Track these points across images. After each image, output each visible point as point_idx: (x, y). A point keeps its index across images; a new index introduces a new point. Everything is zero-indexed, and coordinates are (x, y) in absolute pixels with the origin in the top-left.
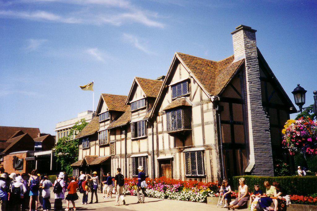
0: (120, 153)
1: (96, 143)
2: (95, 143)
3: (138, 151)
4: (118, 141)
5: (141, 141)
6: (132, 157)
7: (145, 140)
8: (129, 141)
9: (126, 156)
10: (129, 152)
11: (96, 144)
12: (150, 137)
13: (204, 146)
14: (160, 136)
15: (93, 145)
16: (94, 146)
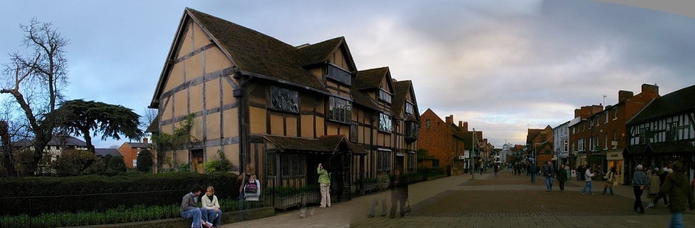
0: (363, 142)
1: (315, 109)
2: (313, 110)
3: (383, 145)
4: (360, 124)
5: (386, 136)
6: (379, 151)
7: (389, 136)
8: (375, 131)
9: (374, 148)
10: (374, 143)
11: (315, 114)
12: (392, 135)
13: (414, 151)
14: (398, 136)
15: (308, 113)
16: (312, 117)
